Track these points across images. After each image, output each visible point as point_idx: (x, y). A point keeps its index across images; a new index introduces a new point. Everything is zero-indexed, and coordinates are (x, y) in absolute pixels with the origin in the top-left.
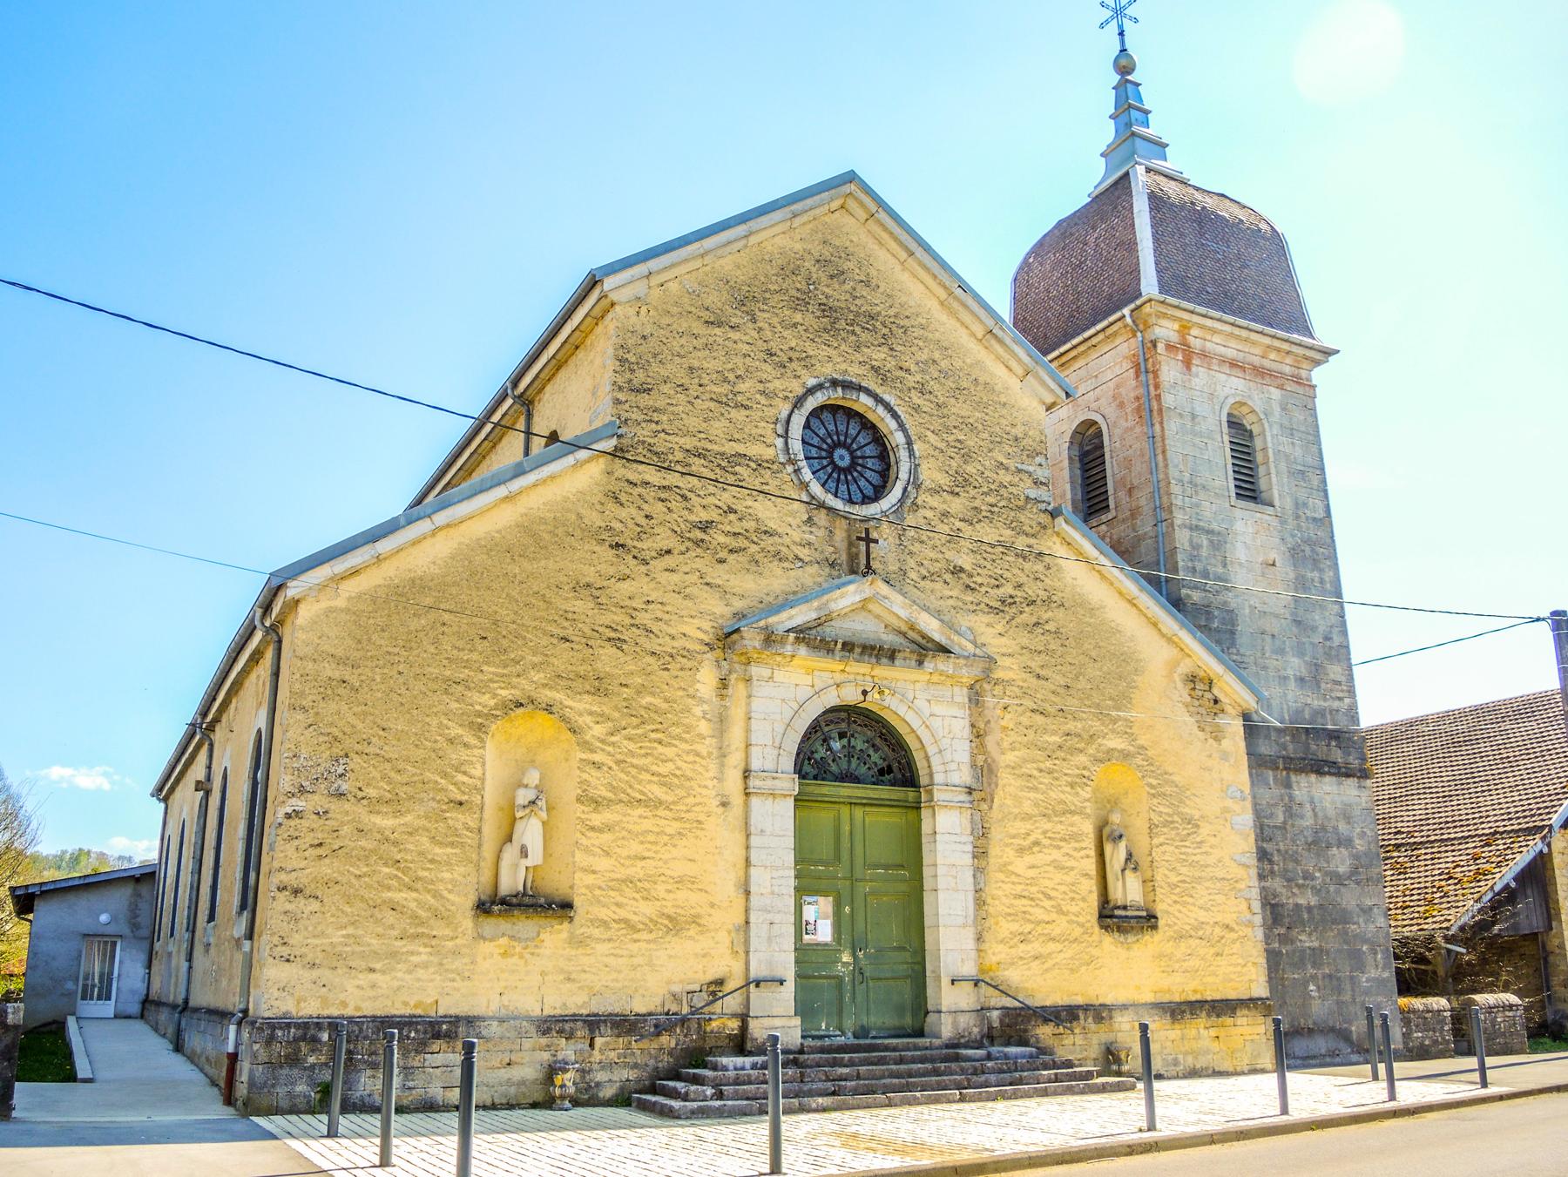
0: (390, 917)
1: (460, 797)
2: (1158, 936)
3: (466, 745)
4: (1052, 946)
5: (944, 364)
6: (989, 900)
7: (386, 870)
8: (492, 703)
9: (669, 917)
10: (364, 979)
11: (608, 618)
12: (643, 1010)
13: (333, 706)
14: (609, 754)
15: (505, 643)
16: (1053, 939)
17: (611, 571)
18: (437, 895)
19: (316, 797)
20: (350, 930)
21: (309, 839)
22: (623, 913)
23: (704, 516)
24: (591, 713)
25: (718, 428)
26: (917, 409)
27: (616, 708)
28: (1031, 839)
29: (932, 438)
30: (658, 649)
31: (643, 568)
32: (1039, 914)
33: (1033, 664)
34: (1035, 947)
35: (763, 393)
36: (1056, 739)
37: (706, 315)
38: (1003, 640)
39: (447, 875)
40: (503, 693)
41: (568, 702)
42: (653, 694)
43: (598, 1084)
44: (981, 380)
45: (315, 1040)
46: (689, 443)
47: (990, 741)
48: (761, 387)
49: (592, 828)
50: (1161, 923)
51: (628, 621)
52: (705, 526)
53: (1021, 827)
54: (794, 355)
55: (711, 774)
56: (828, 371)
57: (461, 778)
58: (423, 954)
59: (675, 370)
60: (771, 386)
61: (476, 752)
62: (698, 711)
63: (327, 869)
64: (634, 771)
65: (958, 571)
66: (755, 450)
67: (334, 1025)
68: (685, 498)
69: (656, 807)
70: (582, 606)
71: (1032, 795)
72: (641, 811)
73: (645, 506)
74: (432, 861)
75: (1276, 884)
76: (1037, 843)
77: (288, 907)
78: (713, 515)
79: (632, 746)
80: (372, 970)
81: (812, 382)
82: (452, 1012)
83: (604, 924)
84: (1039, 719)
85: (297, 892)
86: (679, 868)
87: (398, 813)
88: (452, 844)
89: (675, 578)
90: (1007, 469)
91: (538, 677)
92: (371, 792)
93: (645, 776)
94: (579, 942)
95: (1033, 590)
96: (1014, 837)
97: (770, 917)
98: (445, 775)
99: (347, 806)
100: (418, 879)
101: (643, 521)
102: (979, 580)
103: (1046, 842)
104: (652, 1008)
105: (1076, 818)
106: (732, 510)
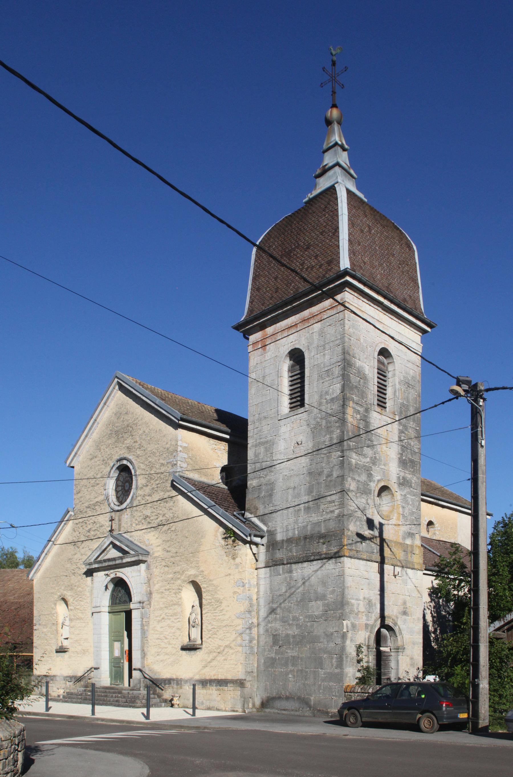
6: (149, 641)
16: (167, 654)
33: (166, 547)
36: (171, 576)
71: (163, 600)
72: (78, 621)
75: (277, 625)
76: (163, 618)
84: (166, 569)
95: (169, 515)
96: (157, 617)
103: (166, 617)
105: (176, 606)
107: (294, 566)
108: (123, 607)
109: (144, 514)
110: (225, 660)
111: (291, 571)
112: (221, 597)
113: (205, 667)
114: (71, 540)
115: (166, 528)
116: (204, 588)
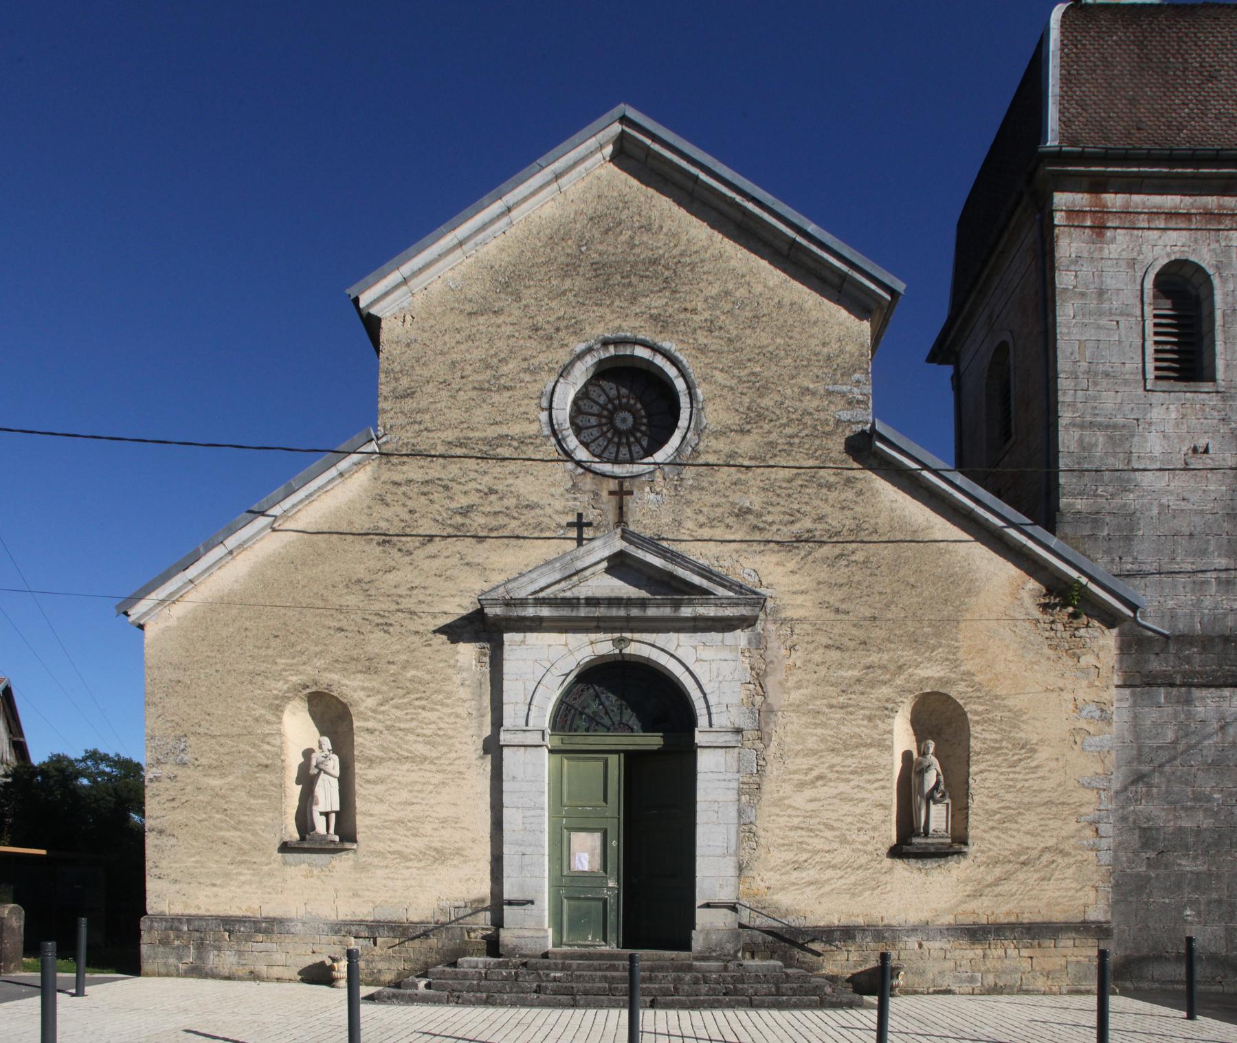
0: (224, 849)
1: (265, 762)
2: (964, 863)
3: (268, 722)
4: (830, 873)
5: (741, 293)
6: (761, 833)
7: (218, 816)
8: (285, 687)
9: (435, 849)
10: (210, 891)
11: (377, 607)
12: (415, 919)
13: (174, 701)
14: (380, 721)
15: (293, 639)
16: (834, 867)
17: (379, 565)
18: (254, 833)
19: (168, 767)
20: (197, 858)
21: (165, 797)
22: (395, 847)
23: (464, 501)
24: (363, 689)
25: (479, 415)
26: (703, 350)
27: (385, 683)
28: (815, 773)
29: (719, 377)
30: (421, 629)
31: (407, 559)
32: (817, 843)
33: (832, 600)
34: (812, 874)
35: (526, 370)
36: (855, 673)
37: (468, 308)
38: (796, 578)
39: (261, 819)
40: (294, 679)
41: (345, 681)
42: (417, 668)
43: (380, 971)
44: (786, 301)
45: (178, 930)
46: (450, 435)
47: (770, 682)
48: (525, 365)
49: (368, 781)
50: (971, 849)
51: (394, 607)
52: (466, 511)
53: (802, 762)
54: (562, 324)
55: (470, 732)
56: (601, 331)
57: (266, 747)
58: (247, 875)
59: (438, 368)
60: (536, 362)
61: (275, 726)
62: (457, 679)
63: (180, 816)
64: (400, 734)
65: (743, 513)
66: (516, 429)
67: (190, 919)
68: (446, 488)
69: (422, 763)
70: (352, 600)
71: (819, 731)
72: (407, 766)
73: (409, 503)
74: (249, 809)
76: (820, 777)
77: (157, 842)
78: (474, 499)
79: (399, 713)
80: (214, 885)
81: (581, 347)
82: (271, 915)
83: (380, 854)
84: (835, 655)
85: (161, 832)
86: (443, 812)
87: (223, 776)
88: (262, 797)
89: (437, 563)
90: (813, 394)
91: (320, 663)
92: (203, 761)
93: (411, 737)
94: (362, 868)
95: (836, 520)
96: (795, 772)
97: (521, 849)
98: (254, 745)
99: (189, 772)
100: (240, 822)
101: (407, 517)
102: (769, 518)
104: (423, 918)
106: (492, 491)
107: (1196, 693)
108: (625, 740)
109: (733, 504)
110: (1043, 879)
111: (1188, 701)
112: (1034, 739)
113: (977, 894)
114: (362, 524)
115: (826, 550)
116: (976, 713)
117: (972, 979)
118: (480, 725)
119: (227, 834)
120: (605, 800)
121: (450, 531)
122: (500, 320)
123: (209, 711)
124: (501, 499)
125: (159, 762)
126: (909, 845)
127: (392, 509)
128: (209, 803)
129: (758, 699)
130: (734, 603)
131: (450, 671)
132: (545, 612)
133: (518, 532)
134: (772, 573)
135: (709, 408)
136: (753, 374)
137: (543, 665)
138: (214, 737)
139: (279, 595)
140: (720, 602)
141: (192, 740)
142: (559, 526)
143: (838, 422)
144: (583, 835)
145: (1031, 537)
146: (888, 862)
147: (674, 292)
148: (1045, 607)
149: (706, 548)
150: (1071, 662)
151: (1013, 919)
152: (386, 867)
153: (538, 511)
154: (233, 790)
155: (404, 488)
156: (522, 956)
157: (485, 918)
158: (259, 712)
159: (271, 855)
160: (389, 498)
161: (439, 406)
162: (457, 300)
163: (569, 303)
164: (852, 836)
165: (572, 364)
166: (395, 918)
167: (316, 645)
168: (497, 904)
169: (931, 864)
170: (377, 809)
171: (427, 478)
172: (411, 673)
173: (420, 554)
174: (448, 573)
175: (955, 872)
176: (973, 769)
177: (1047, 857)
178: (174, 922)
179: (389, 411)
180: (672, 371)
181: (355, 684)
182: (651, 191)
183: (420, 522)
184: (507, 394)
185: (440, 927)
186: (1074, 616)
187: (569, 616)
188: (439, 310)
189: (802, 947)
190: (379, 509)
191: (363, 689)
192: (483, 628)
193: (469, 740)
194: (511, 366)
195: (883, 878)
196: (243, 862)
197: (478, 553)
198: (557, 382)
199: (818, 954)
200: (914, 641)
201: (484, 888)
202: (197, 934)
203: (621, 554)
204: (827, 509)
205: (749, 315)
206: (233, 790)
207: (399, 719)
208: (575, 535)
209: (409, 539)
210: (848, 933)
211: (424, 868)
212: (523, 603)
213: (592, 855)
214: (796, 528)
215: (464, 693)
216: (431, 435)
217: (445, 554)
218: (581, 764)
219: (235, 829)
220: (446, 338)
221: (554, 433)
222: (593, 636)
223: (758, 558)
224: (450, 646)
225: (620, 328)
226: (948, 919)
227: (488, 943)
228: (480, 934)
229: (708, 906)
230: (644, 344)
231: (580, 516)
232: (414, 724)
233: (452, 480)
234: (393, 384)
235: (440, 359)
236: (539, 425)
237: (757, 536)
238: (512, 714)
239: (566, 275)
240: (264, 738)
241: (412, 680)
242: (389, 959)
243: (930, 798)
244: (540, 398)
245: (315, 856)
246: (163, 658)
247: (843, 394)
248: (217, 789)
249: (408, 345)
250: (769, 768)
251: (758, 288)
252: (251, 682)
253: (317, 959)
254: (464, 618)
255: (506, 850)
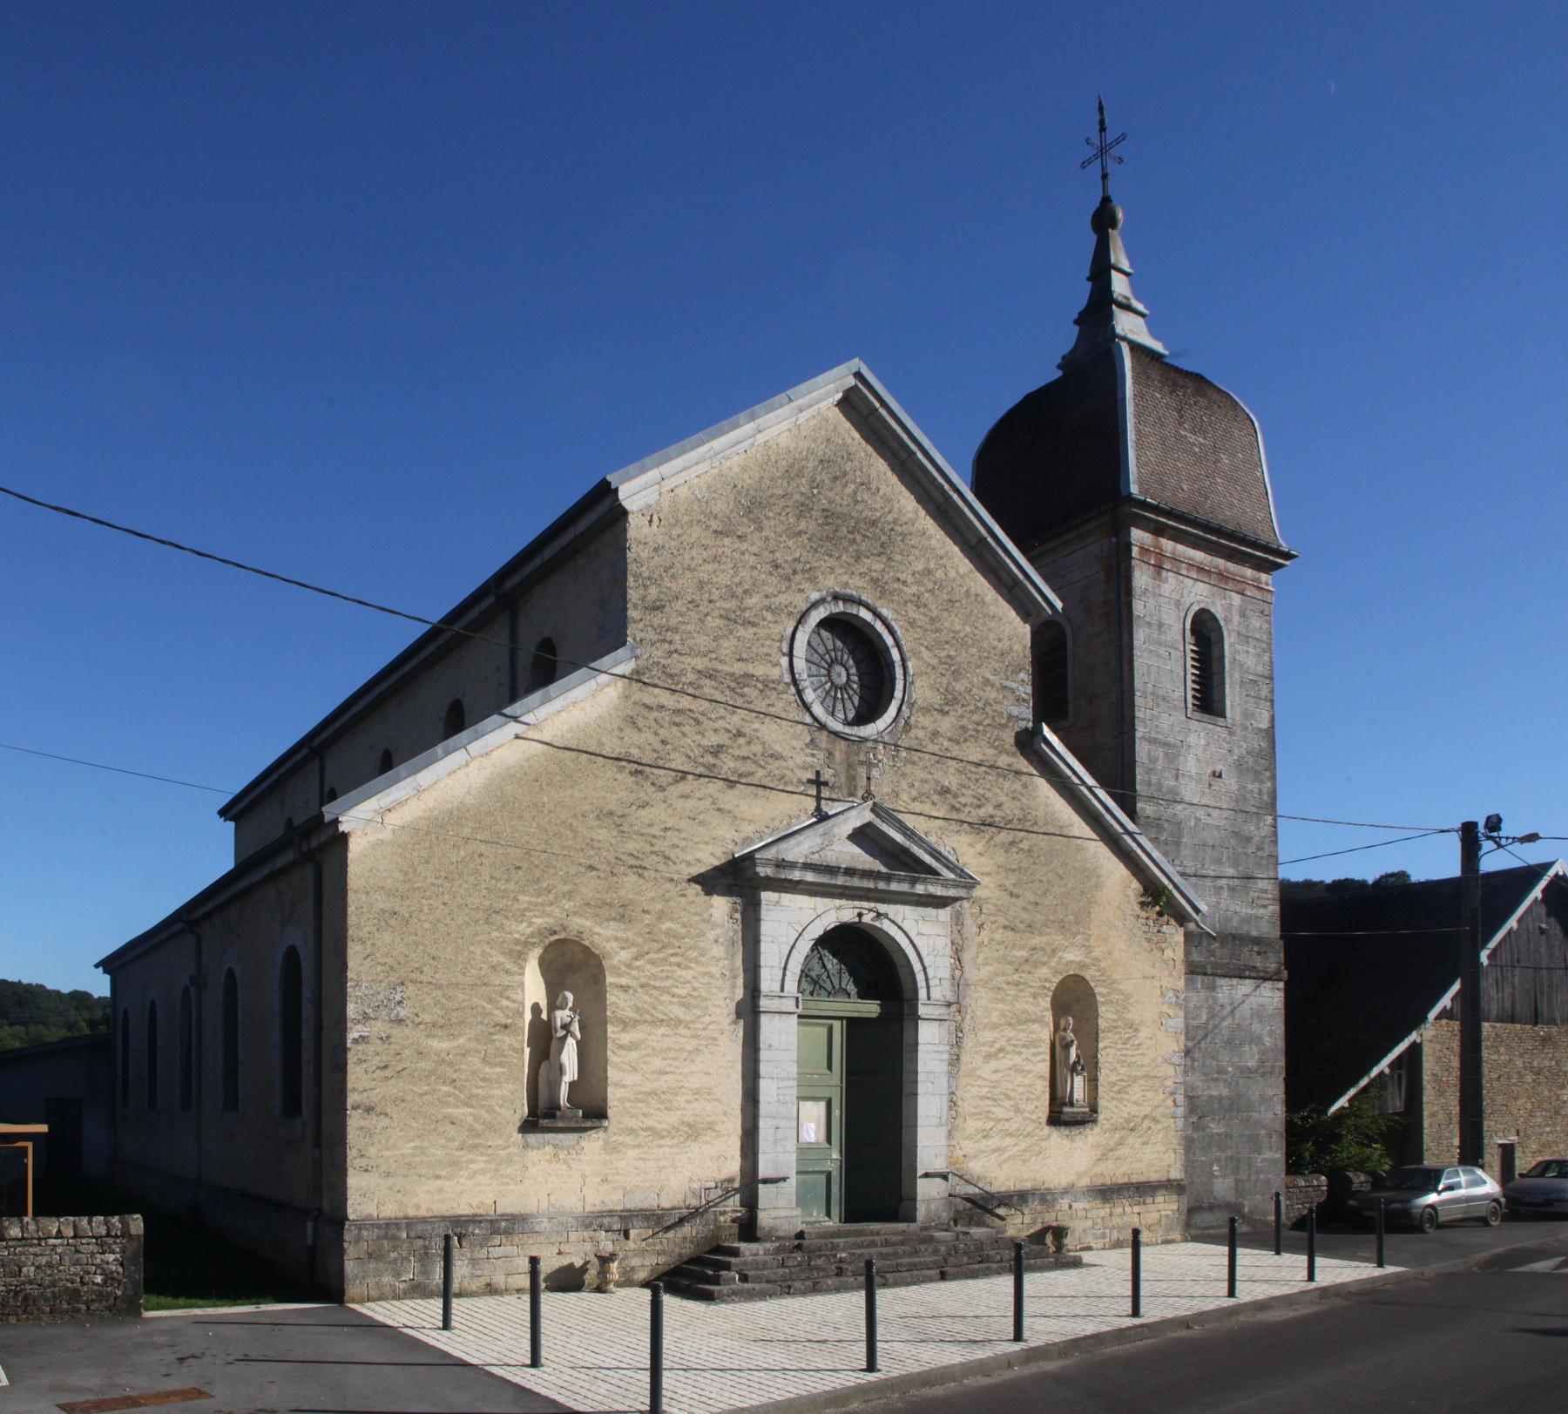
0: (452, 1131)
1: (504, 1021)
2: (1097, 1130)
3: (507, 972)
4: (1009, 1140)
5: (939, 574)
6: (959, 1103)
7: (445, 1089)
8: (529, 931)
9: (689, 1125)
10: (433, 1185)
11: (631, 846)
12: (667, 1205)
13: (387, 937)
14: (634, 978)
15: (537, 873)
16: (1011, 1135)
17: (632, 797)
18: (490, 1110)
19: (379, 1024)
20: (417, 1143)
21: (376, 1061)
22: (649, 1122)
23: (715, 739)
24: (617, 939)
25: (727, 646)
26: (912, 623)
27: (639, 934)
28: (997, 1046)
29: (925, 653)
30: (676, 877)
31: (660, 795)
32: (999, 1112)
34: (994, 1142)
35: (768, 608)
36: (1024, 953)
37: (715, 525)
38: (983, 859)
39: (498, 1092)
40: (538, 921)
41: (597, 929)
42: (672, 920)
43: (633, 1268)
44: (972, 591)
45: (395, 1238)
46: (700, 663)
47: (967, 957)
48: (767, 602)
49: (621, 1047)
50: (1101, 1117)
51: (648, 848)
52: (717, 751)
53: (988, 1035)
54: (799, 567)
55: (723, 995)
56: (831, 583)
57: (505, 1002)
58: (480, 1161)
59: (685, 583)
60: (776, 601)
61: (517, 978)
62: (711, 935)
63: (393, 1088)
64: (655, 993)
65: (945, 791)
66: (759, 670)
67: (410, 1223)
68: (698, 722)
69: (677, 1027)
70: (604, 834)
71: (1000, 1006)
72: (662, 1030)
73: (661, 731)
74: (484, 1080)
76: (1001, 1050)
77: (363, 1123)
78: (722, 738)
79: (654, 970)
80: (438, 1177)
81: (815, 596)
82: (508, 1211)
83: (631, 1131)
85: (369, 1110)
86: (695, 1082)
87: (452, 1036)
88: (501, 1065)
89: (691, 803)
90: (992, 685)
91: (569, 905)
92: (426, 1017)
93: (666, 998)
94: (611, 1148)
95: (1011, 809)
96: (984, 1044)
97: (776, 1122)
98: (490, 1001)
99: (407, 1031)
100: (471, 1096)
101: (659, 746)
102: (963, 799)
103: (1009, 1048)
104: (675, 1203)
105: (1036, 1026)
106: (740, 734)
108: (849, 1007)
109: (937, 782)
110: (1144, 1143)
111: (1213, 988)
112: (1137, 1019)
113: (1103, 1158)
114: (611, 746)
115: (1004, 837)
116: (1103, 995)
117: (1104, 1236)
118: (734, 986)
119: (457, 1112)
120: (830, 1067)
121: (701, 770)
122: (744, 546)
123: (433, 953)
124: (749, 743)
125: (366, 1017)
126: (1061, 1115)
127: (644, 736)
128: (432, 1072)
129: (958, 973)
130: (956, 885)
131: (703, 926)
132: (810, 877)
133: (766, 782)
134: (966, 850)
135: (918, 684)
136: (949, 656)
137: (792, 923)
138: (440, 987)
139: (521, 818)
140: (946, 884)
141: (411, 989)
142: (800, 781)
143: (1010, 716)
144: (809, 1104)
145: (1139, 845)
146: (1047, 1129)
147: (890, 559)
148: (1142, 904)
149: (929, 828)
150: (1159, 954)
151: (1126, 1180)
152: (639, 1146)
153: (781, 762)
154: (464, 1055)
155: (655, 714)
156: (778, 1238)
157: (734, 1202)
158: (498, 958)
159: (510, 1136)
160: (641, 722)
161: (688, 627)
162: (703, 512)
163: (804, 547)
164: (1023, 1106)
165: (808, 610)
166: (645, 1205)
167: (565, 883)
168: (750, 1184)
169: (1075, 1131)
170: (631, 1079)
171: (680, 706)
172: (666, 925)
173: (674, 791)
174: (701, 817)
175: (1090, 1139)
176: (1101, 1045)
177: (1146, 1123)
178: (389, 1228)
179: (638, 623)
180: (889, 641)
181: (609, 933)
182: (870, 449)
183: (672, 756)
184: (752, 630)
185: (695, 1213)
186: (1160, 914)
187: (827, 881)
188: (686, 518)
189: (991, 1212)
190: (629, 733)
191: (617, 939)
192: (739, 880)
193: (722, 1003)
194: (754, 600)
195: (1044, 1144)
196: (475, 1146)
197: (733, 799)
198: (796, 629)
199: (1002, 1218)
200: (1062, 926)
201: (733, 1166)
202: (420, 1242)
203: (869, 825)
204: (1003, 798)
205: (946, 597)
206: (464, 1055)
207: (654, 976)
208: (814, 793)
209: (662, 772)
210: (1017, 1199)
211: (677, 1145)
212: (792, 865)
213: (818, 1125)
214: (982, 812)
215: (718, 951)
216: (682, 659)
217: (698, 795)
218: (810, 1029)
219: (466, 1105)
220: (694, 552)
221: (795, 682)
222: (837, 902)
223: (956, 837)
224: (703, 898)
225: (846, 584)
226: (1085, 1181)
227: (741, 1227)
228: (728, 1217)
229: (927, 1175)
230: (867, 607)
231: (818, 773)
232: (669, 983)
233: (703, 714)
234: (641, 591)
235: (688, 574)
236: (780, 672)
237: (955, 816)
238: (768, 982)
239: (800, 516)
240: (503, 991)
241: (668, 933)
242: (641, 1253)
243: (1073, 1070)
244: (781, 641)
245: (561, 1136)
246: (372, 881)
247: (1013, 691)
248: (444, 1055)
249: (656, 550)
250: (965, 1041)
251: (952, 574)
252: (487, 922)
253: (565, 1261)
254: (716, 869)
255: (762, 1123)
